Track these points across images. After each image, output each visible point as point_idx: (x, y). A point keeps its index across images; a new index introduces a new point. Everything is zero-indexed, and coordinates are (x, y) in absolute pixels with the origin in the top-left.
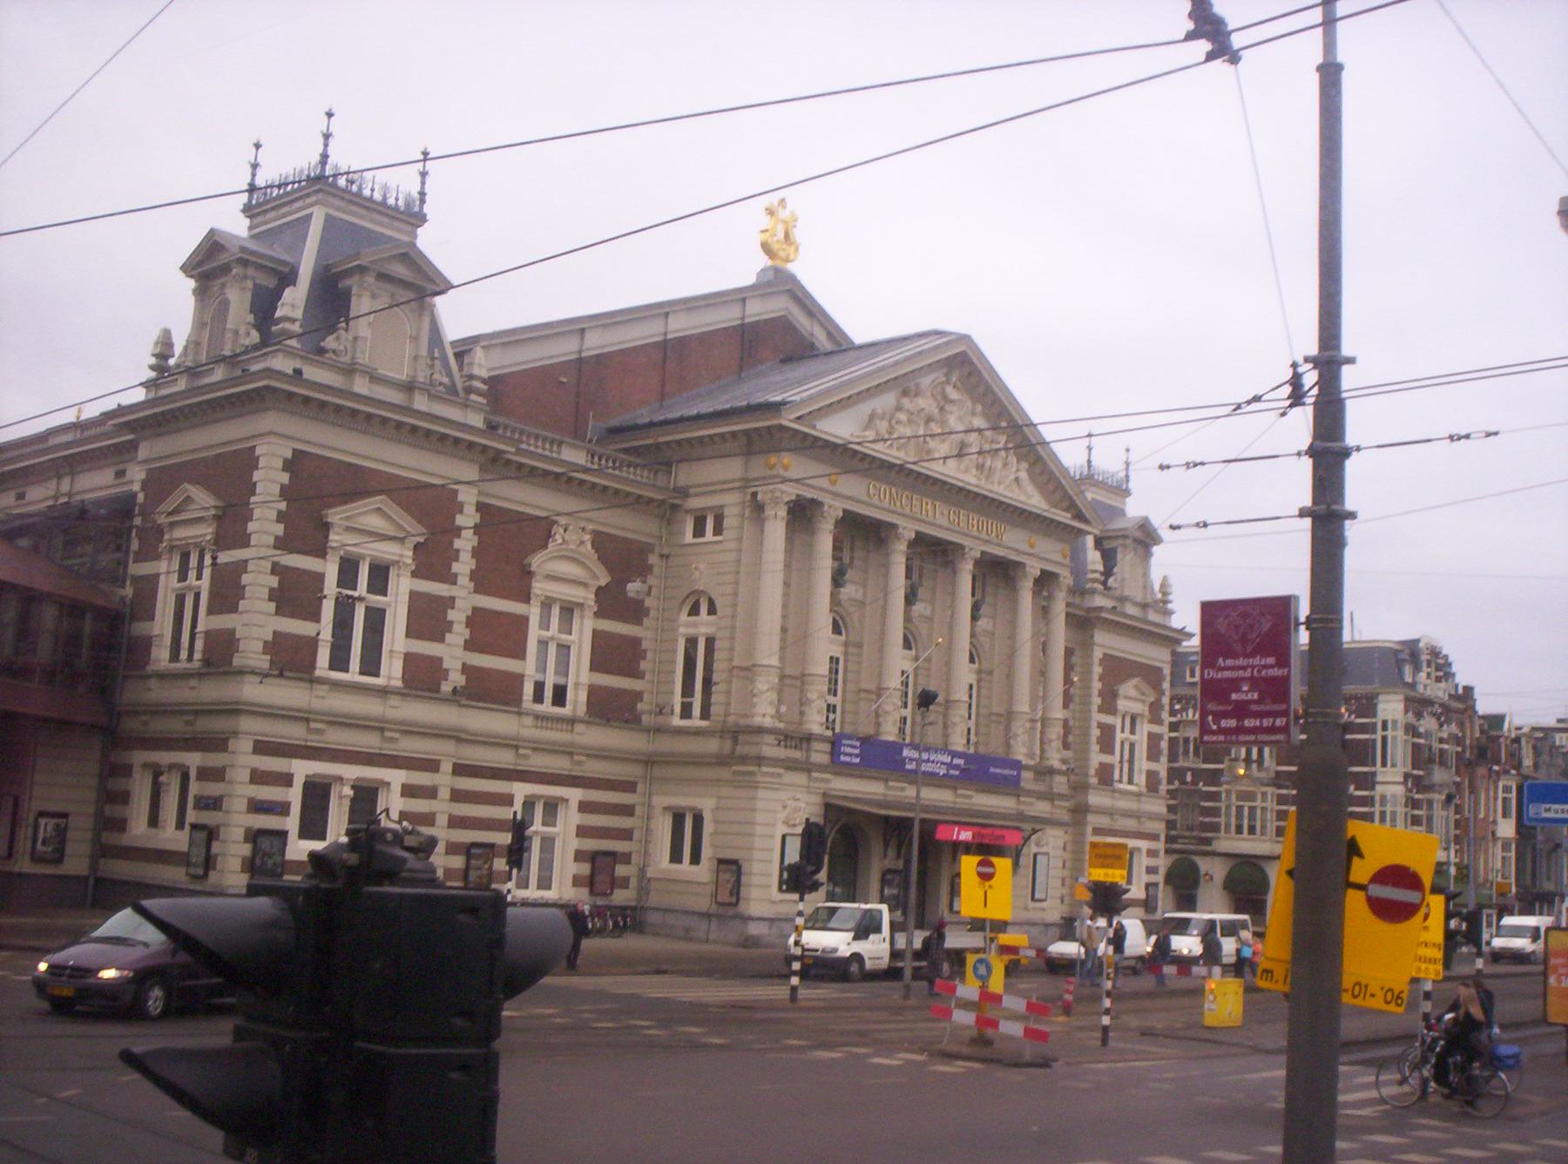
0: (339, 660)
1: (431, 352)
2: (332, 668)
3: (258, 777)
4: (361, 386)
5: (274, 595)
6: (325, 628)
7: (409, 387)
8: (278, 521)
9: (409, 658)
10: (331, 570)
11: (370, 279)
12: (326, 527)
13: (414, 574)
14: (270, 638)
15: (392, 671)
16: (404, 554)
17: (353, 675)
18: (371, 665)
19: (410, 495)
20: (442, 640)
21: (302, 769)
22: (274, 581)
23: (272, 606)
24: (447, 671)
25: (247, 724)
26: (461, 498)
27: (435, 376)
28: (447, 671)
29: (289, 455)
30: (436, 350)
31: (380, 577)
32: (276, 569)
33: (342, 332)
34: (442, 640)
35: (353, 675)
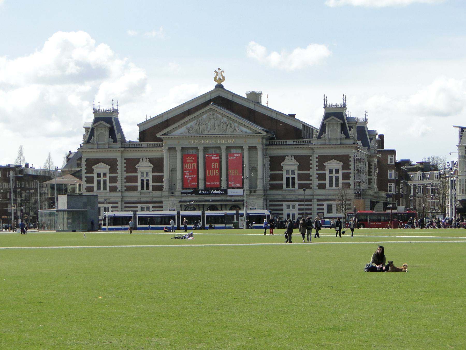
1: (341, 133)
3: (318, 205)
5: (317, 178)
6: (327, 181)
8: (317, 166)
10: (327, 172)
11: (327, 124)
13: (342, 170)
14: (318, 184)
16: (341, 167)
18: (337, 185)
19: (338, 158)
21: (325, 203)
22: (317, 176)
24: (351, 185)
25: (315, 197)
27: (342, 136)
28: (351, 185)
30: (343, 132)
31: (337, 171)
32: (317, 174)
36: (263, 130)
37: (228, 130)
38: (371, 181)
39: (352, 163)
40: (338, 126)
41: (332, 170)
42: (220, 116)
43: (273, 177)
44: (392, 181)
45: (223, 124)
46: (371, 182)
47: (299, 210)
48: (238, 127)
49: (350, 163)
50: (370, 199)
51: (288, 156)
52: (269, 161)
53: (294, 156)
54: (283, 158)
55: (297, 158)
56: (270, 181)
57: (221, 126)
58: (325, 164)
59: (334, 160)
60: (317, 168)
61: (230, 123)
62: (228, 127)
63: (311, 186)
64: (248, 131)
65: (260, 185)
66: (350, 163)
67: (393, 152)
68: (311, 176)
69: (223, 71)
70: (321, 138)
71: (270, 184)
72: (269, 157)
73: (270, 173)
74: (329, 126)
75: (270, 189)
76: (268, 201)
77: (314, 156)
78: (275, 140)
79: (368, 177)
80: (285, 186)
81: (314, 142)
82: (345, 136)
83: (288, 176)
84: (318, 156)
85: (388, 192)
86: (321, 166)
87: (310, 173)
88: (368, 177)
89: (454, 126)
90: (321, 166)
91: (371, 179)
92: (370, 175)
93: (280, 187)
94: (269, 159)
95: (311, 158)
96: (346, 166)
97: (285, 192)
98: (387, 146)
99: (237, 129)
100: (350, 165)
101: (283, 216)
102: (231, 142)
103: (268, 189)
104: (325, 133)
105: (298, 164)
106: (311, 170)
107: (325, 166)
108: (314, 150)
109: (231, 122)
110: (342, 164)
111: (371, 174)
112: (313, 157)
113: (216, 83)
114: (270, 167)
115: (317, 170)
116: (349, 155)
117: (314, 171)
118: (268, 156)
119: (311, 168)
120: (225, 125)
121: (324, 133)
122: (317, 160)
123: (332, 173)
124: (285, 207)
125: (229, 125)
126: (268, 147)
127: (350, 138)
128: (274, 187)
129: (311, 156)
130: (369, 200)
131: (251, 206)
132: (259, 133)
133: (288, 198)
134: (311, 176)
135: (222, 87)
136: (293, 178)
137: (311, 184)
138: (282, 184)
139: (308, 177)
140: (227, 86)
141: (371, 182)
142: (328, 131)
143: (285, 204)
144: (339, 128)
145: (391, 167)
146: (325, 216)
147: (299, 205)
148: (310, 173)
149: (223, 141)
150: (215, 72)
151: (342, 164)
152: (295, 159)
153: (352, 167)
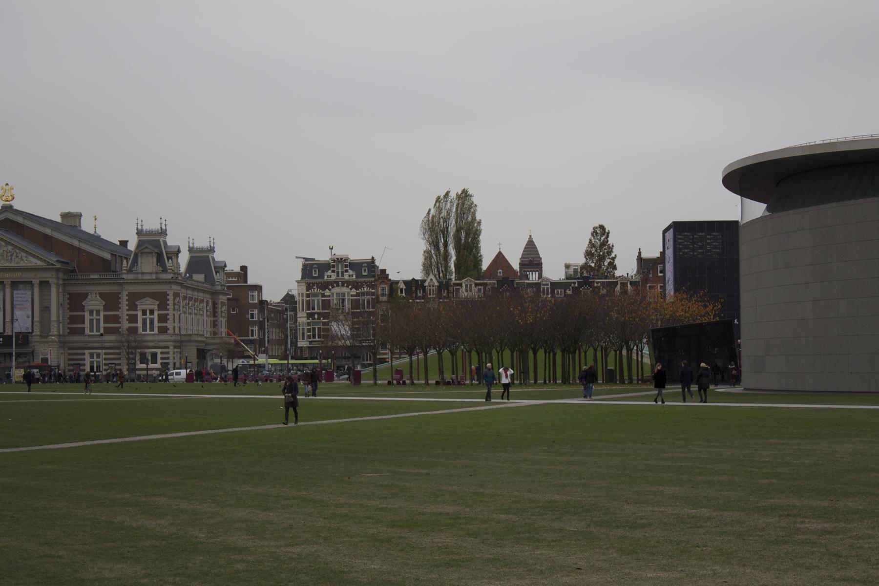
0: (145, 329)
1: (157, 265)
2: (143, 331)
4: (140, 276)
5: (127, 320)
6: (140, 324)
7: (151, 273)
9: (159, 328)
10: (140, 313)
11: (139, 254)
12: (137, 305)
13: (158, 310)
15: (156, 330)
16: (156, 307)
17: (148, 332)
18: (152, 329)
20: (166, 322)
22: (127, 317)
23: (127, 322)
26: (168, 293)
29: (127, 293)
31: (152, 312)
32: (127, 315)
33: (136, 267)
34: (166, 322)
35: (148, 332)
36: (57, 261)
37: (13, 260)
38: (216, 323)
39: (170, 302)
40: (152, 257)
41: (146, 311)
42: (3, 244)
43: (73, 320)
44: (254, 323)
45: (7, 253)
46: (217, 325)
47: (105, 359)
48: (26, 257)
49: (168, 302)
50: (197, 346)
51: (91, 293)
52: (68, 299)
53: (99, 293)
54: (85, 296)
55: (102, 295)
56: (69, 324)
57: (5, 256)
58: (137, 303)
59: (148, 298)
60: (127, 307)
61: (16, 252)
62: (13, 257)
63: (120, 330)
64: (39, 263)
65: (54, 331)
66: (168, 302)
67: (258, 288)
68: (120, 318)
69: (12, 189)
70: (132, 271)
71: (69, 328)
72: (68, 294)
73: (69, 314)
74: (141, 257)
75: (69, 333)
76: (66, 349)
77: (124, 293)
78: (76, 272)
79: (212, 319)
80: (87, 331)
81: (125, 276)
82: (161, 269)
83: (91, 317)
84: (129, 293)
85: (249, 337)
86: (132, 306)
87: (118, 315)
88: (212, 319)
89: (297, 257)
90: (132, 306)
91: (216, 321)
92: (214, 316)
93: (81, 331)
94: (68, 296)
95: (120, 296)
96: (163, 306)
97: (87, 337)
98: (251, 281)
99: (25, 259)
100: (168, 305)
101: (85, 368)
102: (17, 277)
103: (67, 333)
104: (137, 265)
105: (104, 303)
106: (120, 310)
107: (137, 305)
108: (124, 286)
109: (18, 251)
110: (158, 303)
111: (216, 314)
112: (122, 294)
113: (4, 203)
114: (68, 306)
115: (127, 310)
116: (166, 292)
117: (124, 312)
118: (66, 294)
119: (120, 308)
120: (9, 255)
121: (136, 264)
122: (127, 298)
123: (146, 315)
124: (87, 357)
125: (15, 254)
126: (66, 282)
127: (167, 271)
128: (73, 332)
129: (120, 293)
130: (195, 348)
131: (42, 355)
132: (53, 265)
133: (91, 345)
134: (120, 318)
135: (11, 207)
136: (98, 321)
137: (120, 327)
138: (84, 328)
139: (116, 319)
140: (17, 205)
141: (217, 325)
142: (141, 263)
143: (87, 352)
144: (155, 260)
145: (254, 306)
146: (137, 367)
147: (105, 354)
148: (118, 315)
149: (7, 275)
150: (2, 189)
151: (158, 303)
152: (100, 297)
153: (170, 307)
